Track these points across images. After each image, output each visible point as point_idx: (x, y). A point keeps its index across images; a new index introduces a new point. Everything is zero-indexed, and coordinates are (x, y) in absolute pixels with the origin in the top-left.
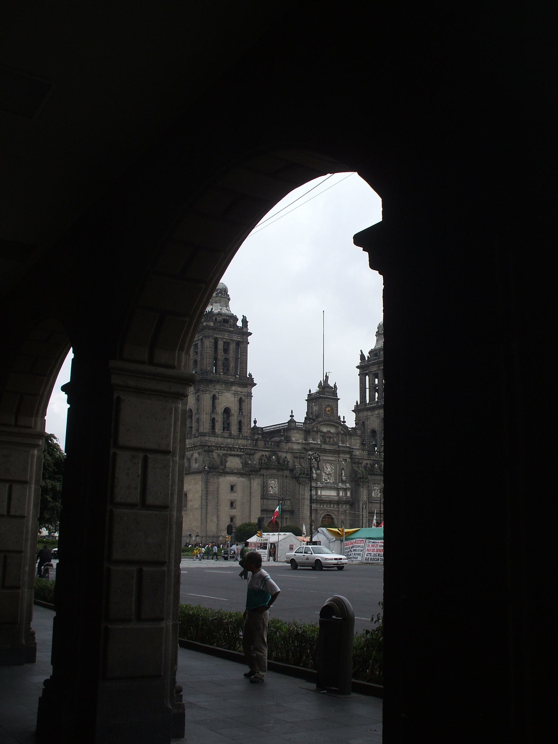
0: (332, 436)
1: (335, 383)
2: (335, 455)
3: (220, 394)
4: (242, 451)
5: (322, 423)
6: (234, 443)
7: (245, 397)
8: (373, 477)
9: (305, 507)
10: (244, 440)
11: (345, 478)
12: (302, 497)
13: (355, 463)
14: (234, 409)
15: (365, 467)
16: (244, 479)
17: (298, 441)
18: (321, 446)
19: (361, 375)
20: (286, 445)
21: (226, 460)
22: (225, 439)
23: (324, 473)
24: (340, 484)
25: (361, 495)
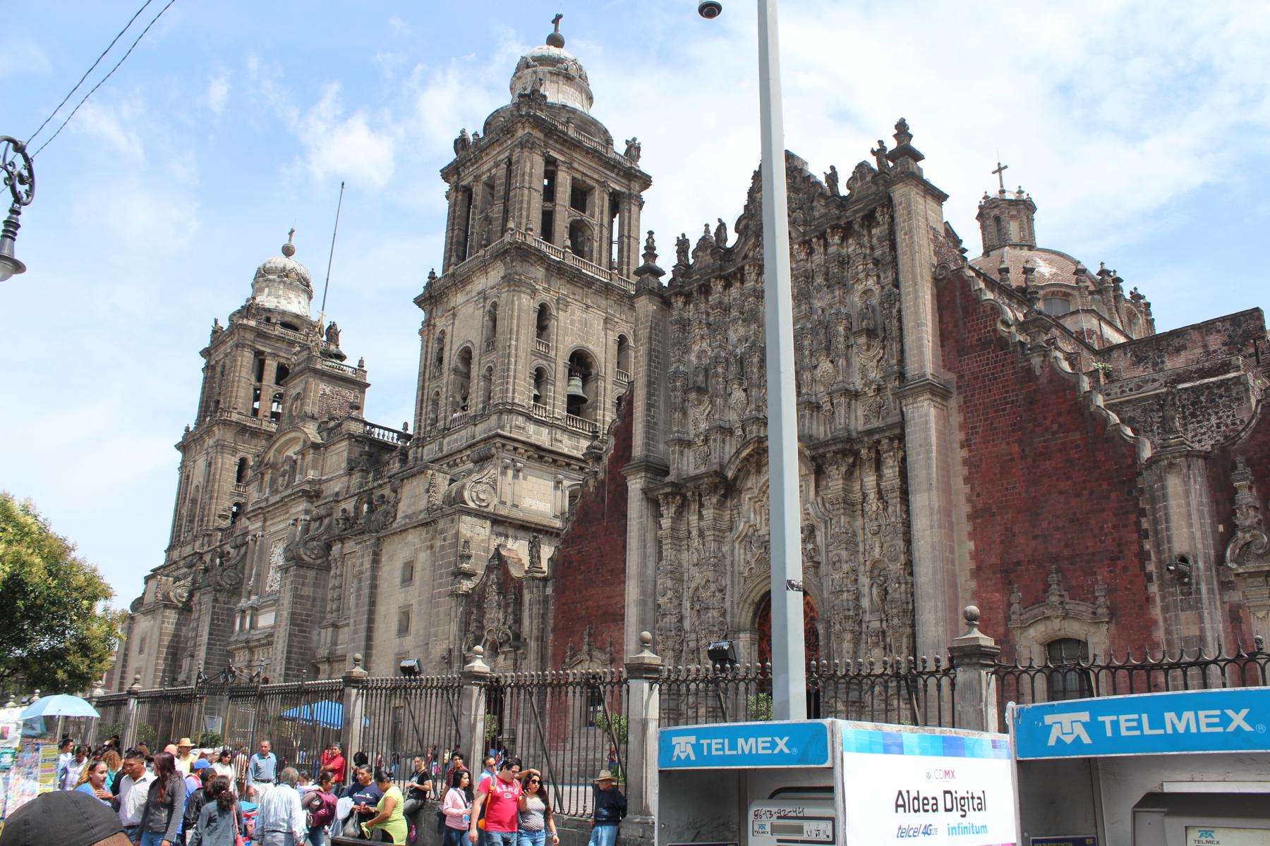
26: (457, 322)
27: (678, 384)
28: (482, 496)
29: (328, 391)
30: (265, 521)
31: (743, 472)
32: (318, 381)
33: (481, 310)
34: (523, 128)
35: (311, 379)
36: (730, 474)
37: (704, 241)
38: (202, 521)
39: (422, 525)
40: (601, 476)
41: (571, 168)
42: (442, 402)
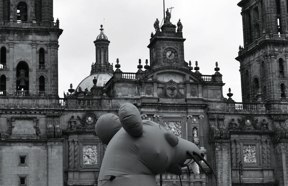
0: (175, 86)
1: (180, 20)
3: (10, 46)
4: (42, 113)
5: (160, 72)
6: (32, 105)
7: (47, 46)
10: (47, 99)
11: (198, 139)
13: (213, 119)
14: (33, 62)
15: (231, 124)
17: (126, 97)
18: (159, 101)
19: (243, 14)
20: (109, 102)
21: (11, 125)
22: (19, 100)
25: (219, 160)
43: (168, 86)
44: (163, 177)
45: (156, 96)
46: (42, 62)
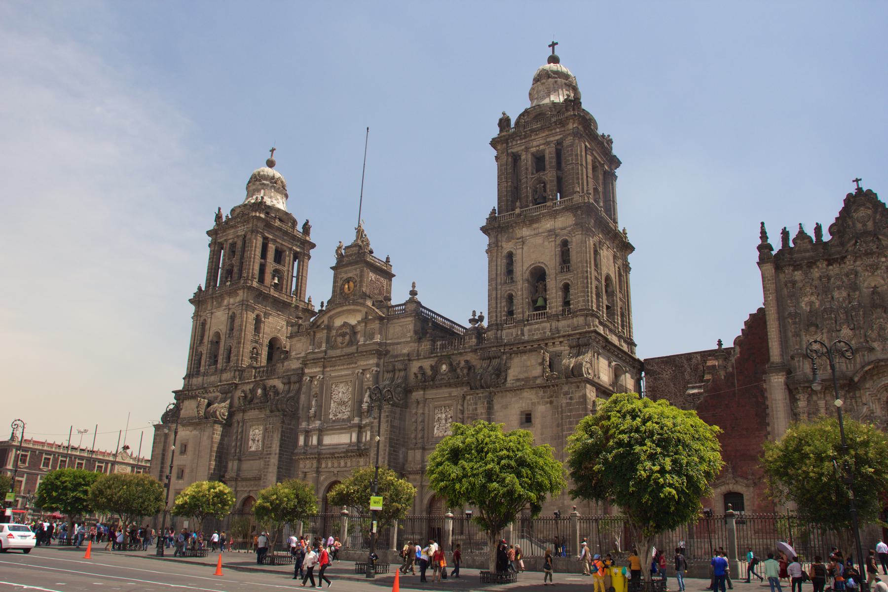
0: (348, 331)
2: (351, 366)
8: (431, 393)
9: (270, 470)
12: (267, 451)
16: (198, 433)
17: (299, 356)
20: (283, 367)
23: (334, 402)
24: (356, 420)
26: (525, 248)
27: (797, 320)
28: (590, 371)
29: (373, 277)
30: (324, 367)
31: (863, 379)
32: (369, 270)
33: (553, 244)
34: (573, 123)
35: (365, 269)
36: (856, 379)
37: (802, 234)
38: (228, 358)
39: (539, 387)
40: (730, 369)
41: (592, 154)
42: (518, 301)
43: (340, 331)
44: (323, 465)
45: (323, 348)
46: (232, 329)
